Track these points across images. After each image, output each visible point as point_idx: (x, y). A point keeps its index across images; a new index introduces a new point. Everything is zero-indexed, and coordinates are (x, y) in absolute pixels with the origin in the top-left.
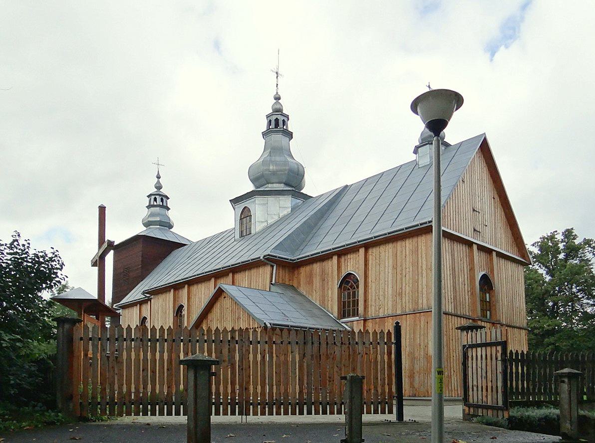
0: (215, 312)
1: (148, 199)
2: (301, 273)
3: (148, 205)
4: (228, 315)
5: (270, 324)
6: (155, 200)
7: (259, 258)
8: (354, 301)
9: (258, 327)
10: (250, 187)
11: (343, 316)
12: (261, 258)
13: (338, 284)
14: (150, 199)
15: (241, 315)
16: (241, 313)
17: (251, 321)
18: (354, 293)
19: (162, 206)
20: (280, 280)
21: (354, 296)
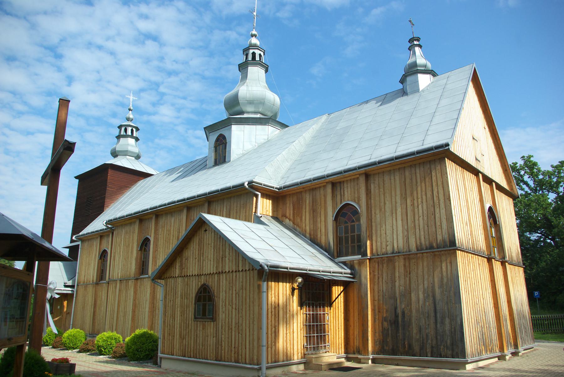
0: (192, 248)
1: (118, 130)
2: (287, 204)
3: (117, 134)
4: (210, 253)
5: (267, 266)
6: (126, 130)
7: (243, 185)
8: (353, 237)
9: (249, 270)
10: (225, 116)
11: (340, 255)
12: (246, 184)
13: (333, 217)
14: (121, 129)
15: (227, 253)
16: (227, 250)
17: (240, 262)
18: (353, 227)
19: (132, 136)
20: (265, 211)
21: (353, 231)
